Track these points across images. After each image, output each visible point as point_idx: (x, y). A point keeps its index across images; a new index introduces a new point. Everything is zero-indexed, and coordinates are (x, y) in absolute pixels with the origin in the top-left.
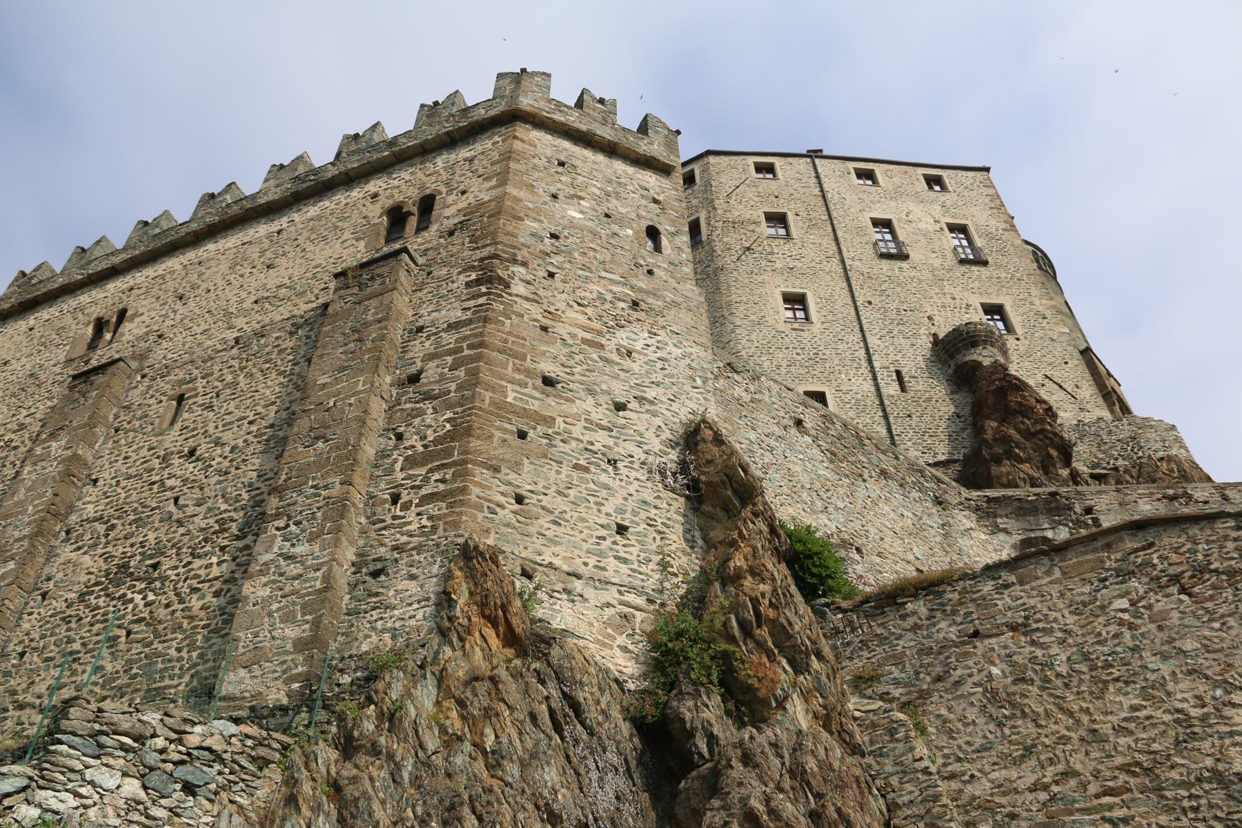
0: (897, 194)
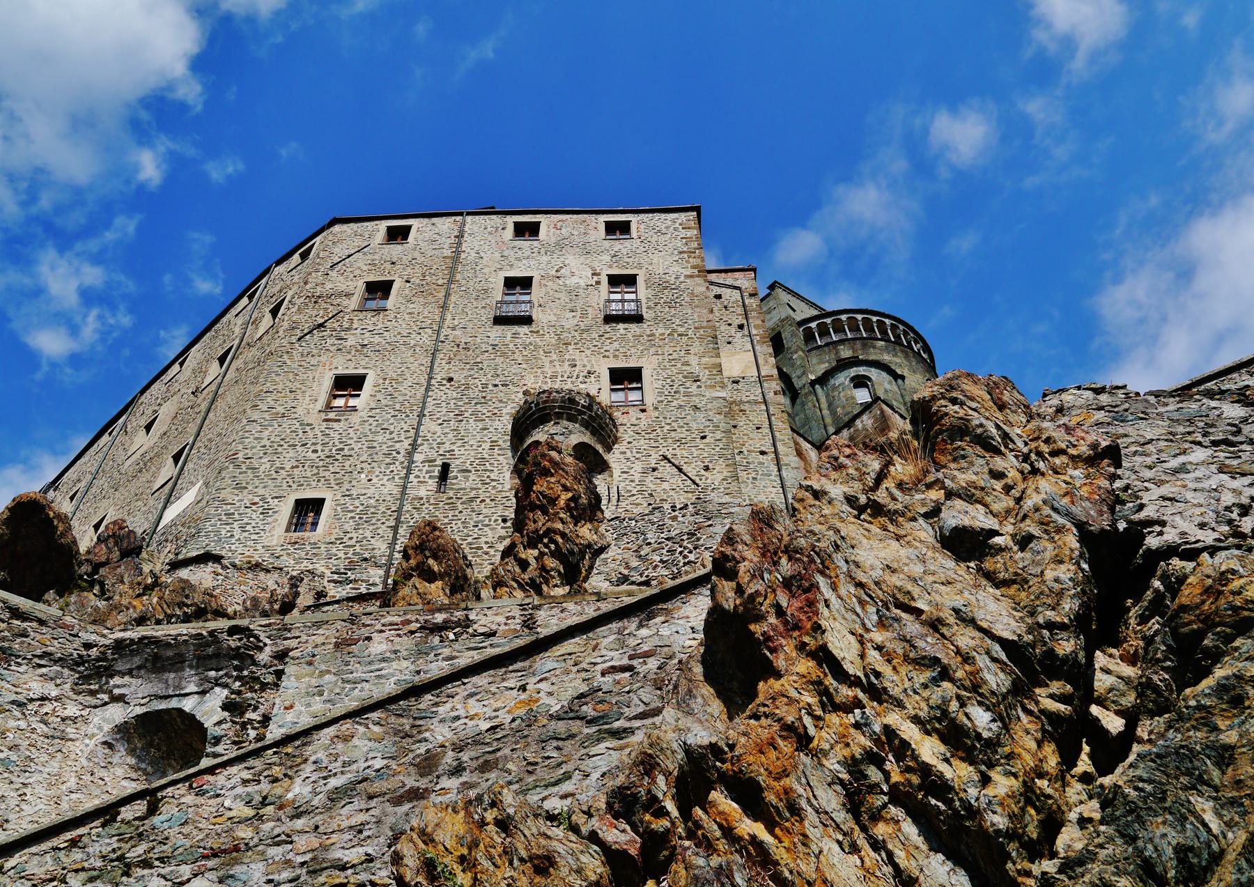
0: (560, 245)
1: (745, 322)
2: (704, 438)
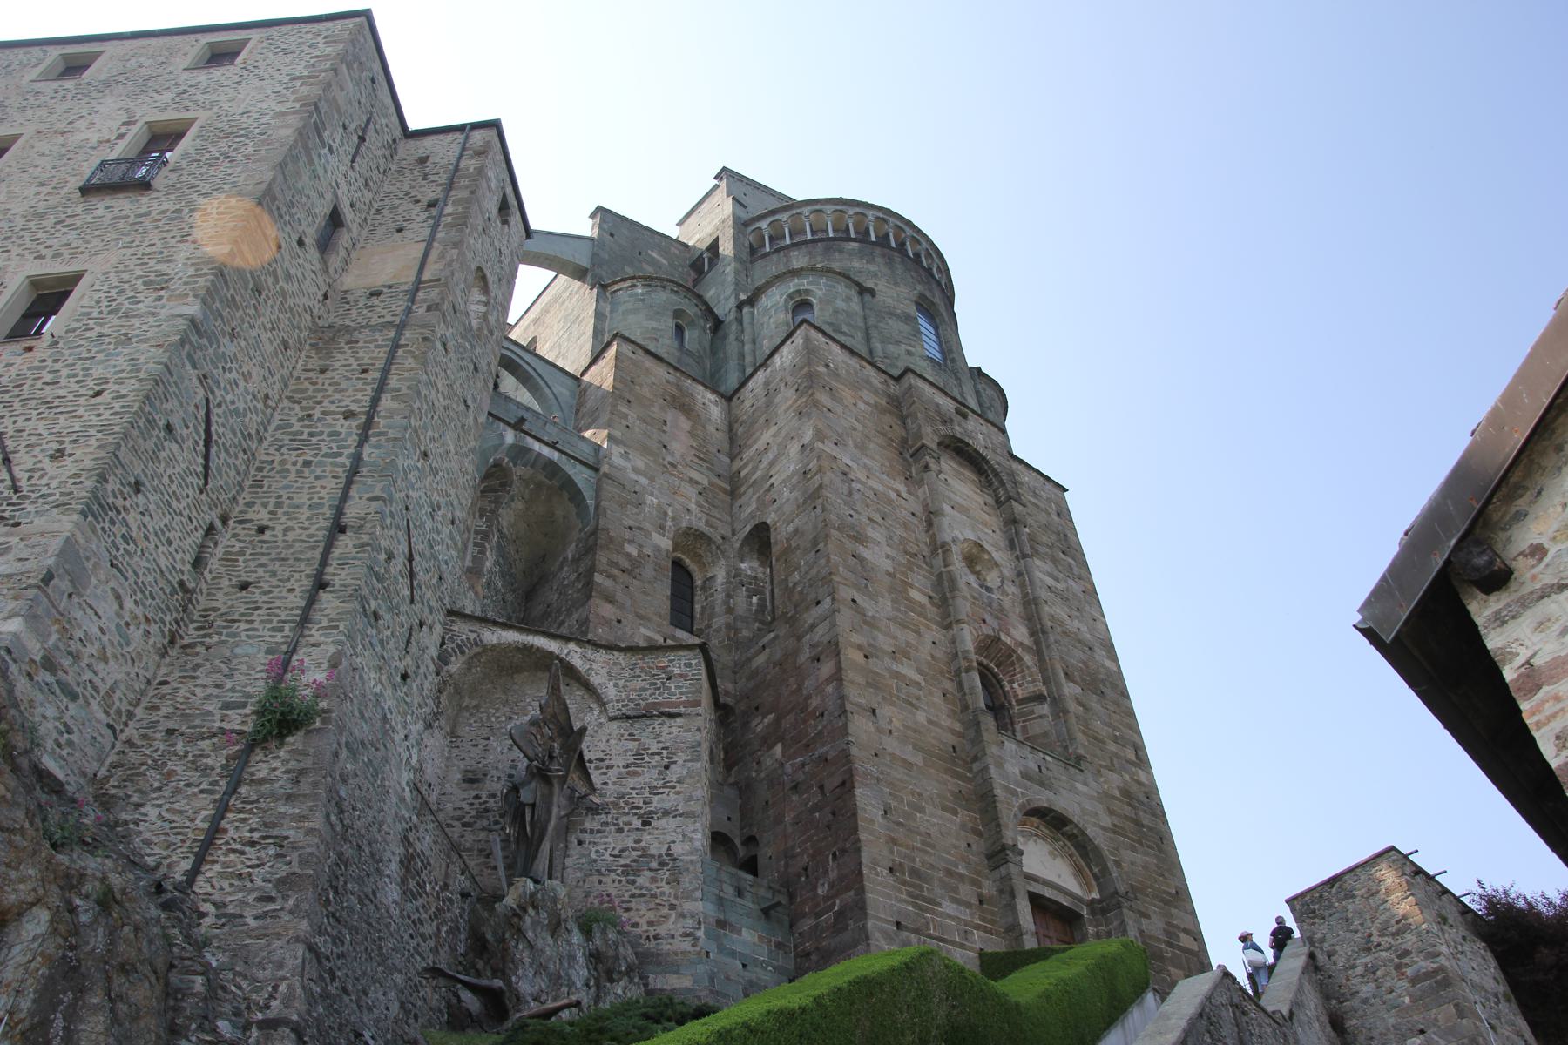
1: (441, 196)
2: (98, 394)
